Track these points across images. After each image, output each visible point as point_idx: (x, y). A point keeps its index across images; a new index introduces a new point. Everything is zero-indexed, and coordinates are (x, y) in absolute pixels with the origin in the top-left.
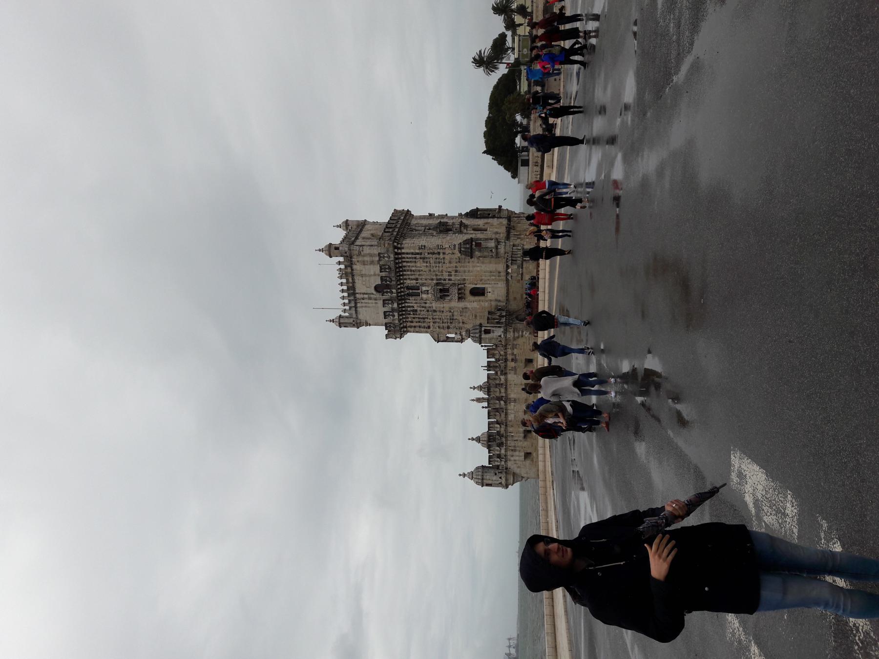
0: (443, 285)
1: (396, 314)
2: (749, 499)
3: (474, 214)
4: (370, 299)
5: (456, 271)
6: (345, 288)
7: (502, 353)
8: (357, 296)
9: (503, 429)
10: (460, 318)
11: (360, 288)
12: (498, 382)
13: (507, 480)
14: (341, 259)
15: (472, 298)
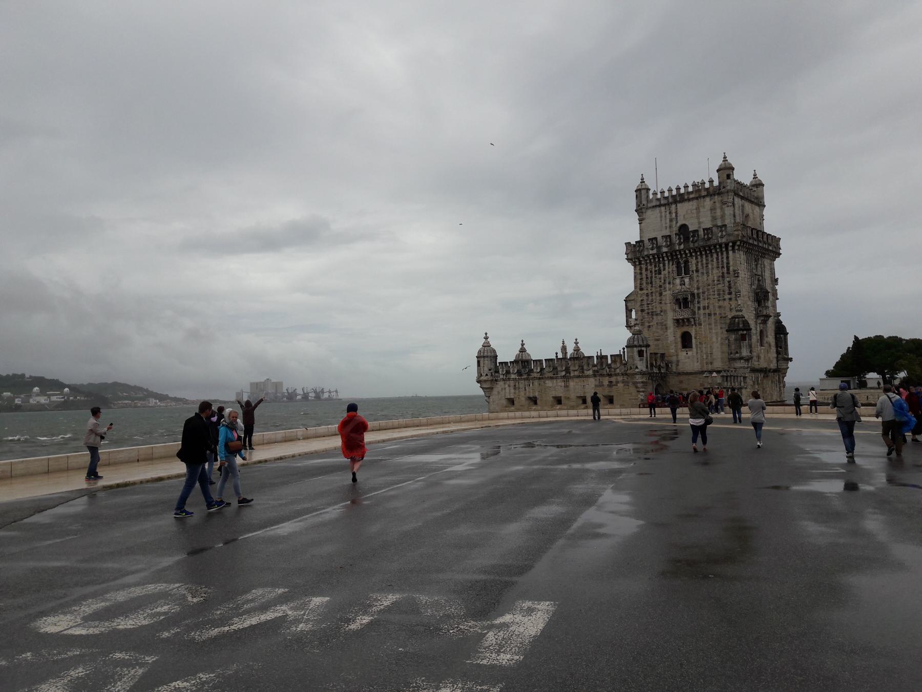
0: (692, 302)
1: (655, 251)
2: (507, 618)
3: (781, 331)
4: (671, 220)
5: (710, 315)
6: (682, 191)
7: (618, 371)
8: (673, 206)
9: (535, 375)
10: (654, 323)
11: (683, 208)
12: (585, 367)
13: (485, 381)
14: (716, 183)
15: (679, 334)
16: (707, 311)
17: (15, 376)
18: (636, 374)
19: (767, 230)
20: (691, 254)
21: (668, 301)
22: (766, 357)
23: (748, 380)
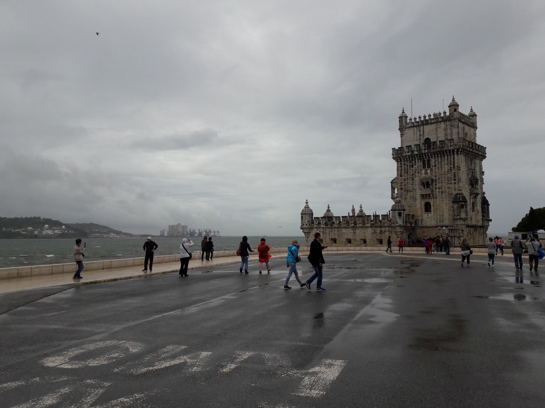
0: (432, 184)
1: (410, 154)
2: (317, 369)
4: (420, 135)
5: (442, 192)
6: (427, 118)
7: (386, 224)
8: (422, 127)
9: (336, 225)
11: (427, 128)
12: (366, 222)
13: (306, 228)
14: (448, 114)
15: (423, 203)
17: (35, 218)
18: (397, 226)
19: (478, 142)
20: (432, 156)
21: (417, 184)
22: (476, 219)
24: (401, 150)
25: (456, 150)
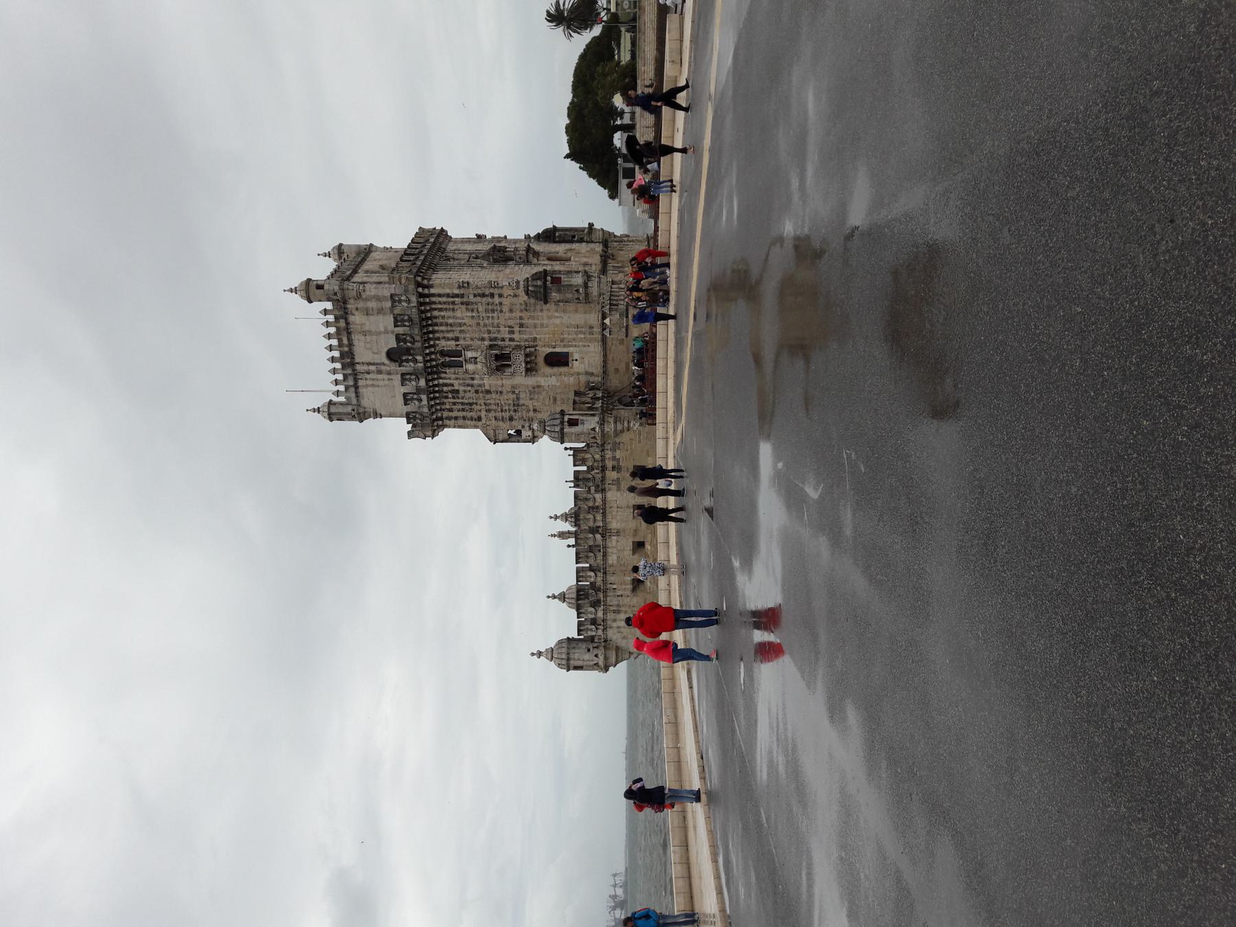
0: (502, 348)
1: (424, 397)
4: (380, 372)
5: (521, 326)
6: (336, 354)
7: (597, 457)
9: (599, 579)
11: (363, 354)
12: (591, 504)
13: (606, 658)
14: (328, 305)
15: (548, 370)
16: (517, 329)
18: (603, 431)
20: (431, 346)
21: (499, 383)
23: (616, 279)
24: (415, 418)
25: (420, 290)
